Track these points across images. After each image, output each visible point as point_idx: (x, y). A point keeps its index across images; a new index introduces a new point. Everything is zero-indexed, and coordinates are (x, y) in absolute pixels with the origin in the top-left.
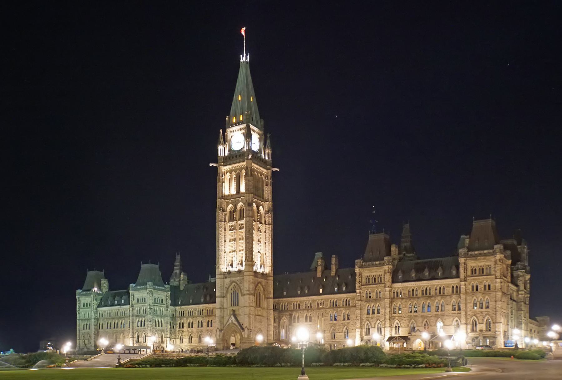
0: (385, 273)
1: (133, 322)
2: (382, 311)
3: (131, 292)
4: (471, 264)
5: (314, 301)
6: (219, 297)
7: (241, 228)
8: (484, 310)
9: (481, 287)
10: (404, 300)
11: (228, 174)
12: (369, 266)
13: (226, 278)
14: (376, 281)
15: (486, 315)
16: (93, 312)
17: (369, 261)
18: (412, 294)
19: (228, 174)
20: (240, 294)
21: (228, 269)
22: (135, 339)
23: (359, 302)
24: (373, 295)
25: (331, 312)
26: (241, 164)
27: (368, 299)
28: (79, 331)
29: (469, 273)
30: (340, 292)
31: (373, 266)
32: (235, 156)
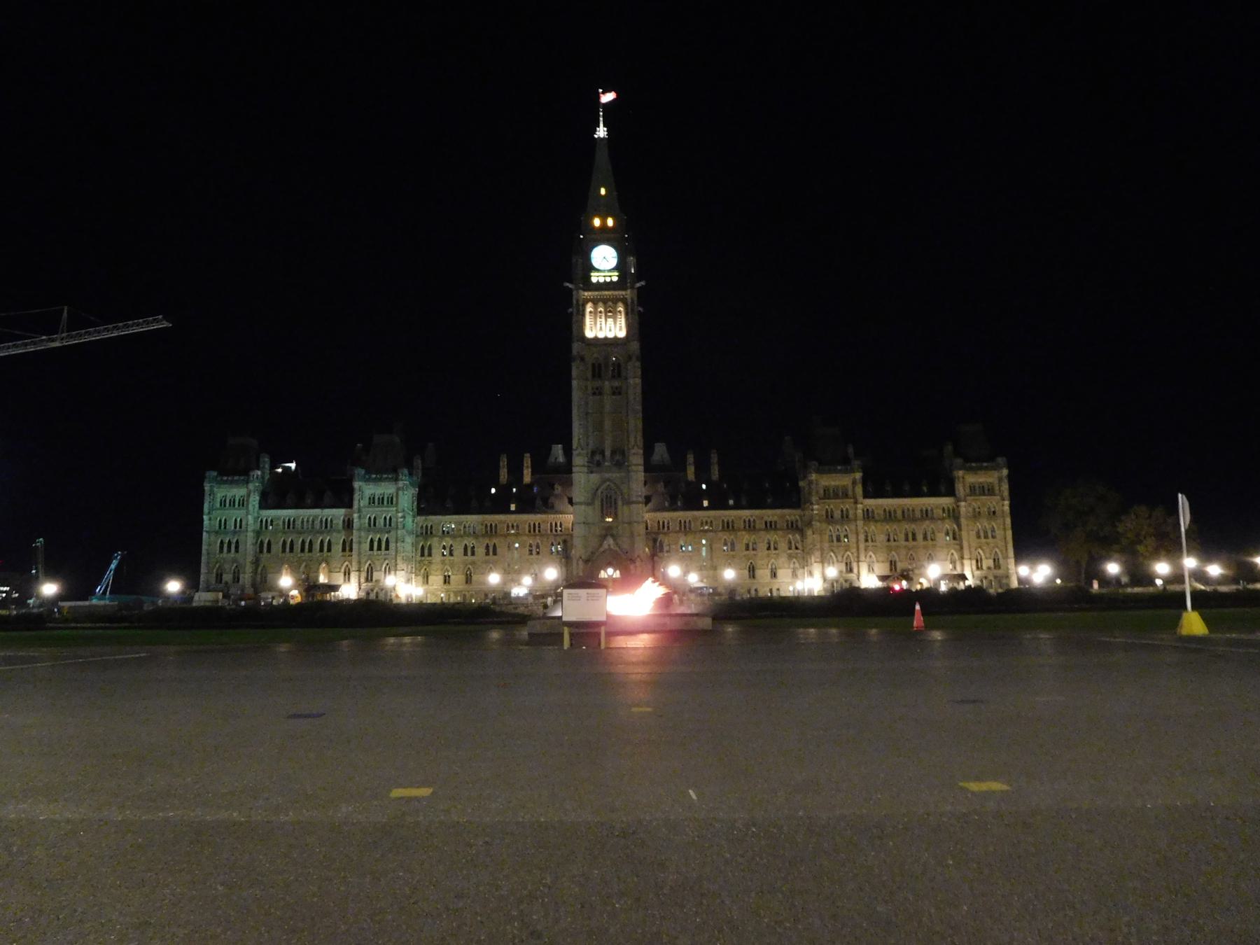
0: (854, 483)
1: (360, 543)
4: (971, 479)
5: (696, 519)
8: (990, 540)
10: (879, 524)
12: (829, 472)
17: (827, 465)
18: (889, 517)
20: (620, 503)
24: (837, 514)
25: (725, 536)
26: (616, 293)
27: (829, 518)
29: (968, 491)
30: (736, 507)
31: (836, 471)
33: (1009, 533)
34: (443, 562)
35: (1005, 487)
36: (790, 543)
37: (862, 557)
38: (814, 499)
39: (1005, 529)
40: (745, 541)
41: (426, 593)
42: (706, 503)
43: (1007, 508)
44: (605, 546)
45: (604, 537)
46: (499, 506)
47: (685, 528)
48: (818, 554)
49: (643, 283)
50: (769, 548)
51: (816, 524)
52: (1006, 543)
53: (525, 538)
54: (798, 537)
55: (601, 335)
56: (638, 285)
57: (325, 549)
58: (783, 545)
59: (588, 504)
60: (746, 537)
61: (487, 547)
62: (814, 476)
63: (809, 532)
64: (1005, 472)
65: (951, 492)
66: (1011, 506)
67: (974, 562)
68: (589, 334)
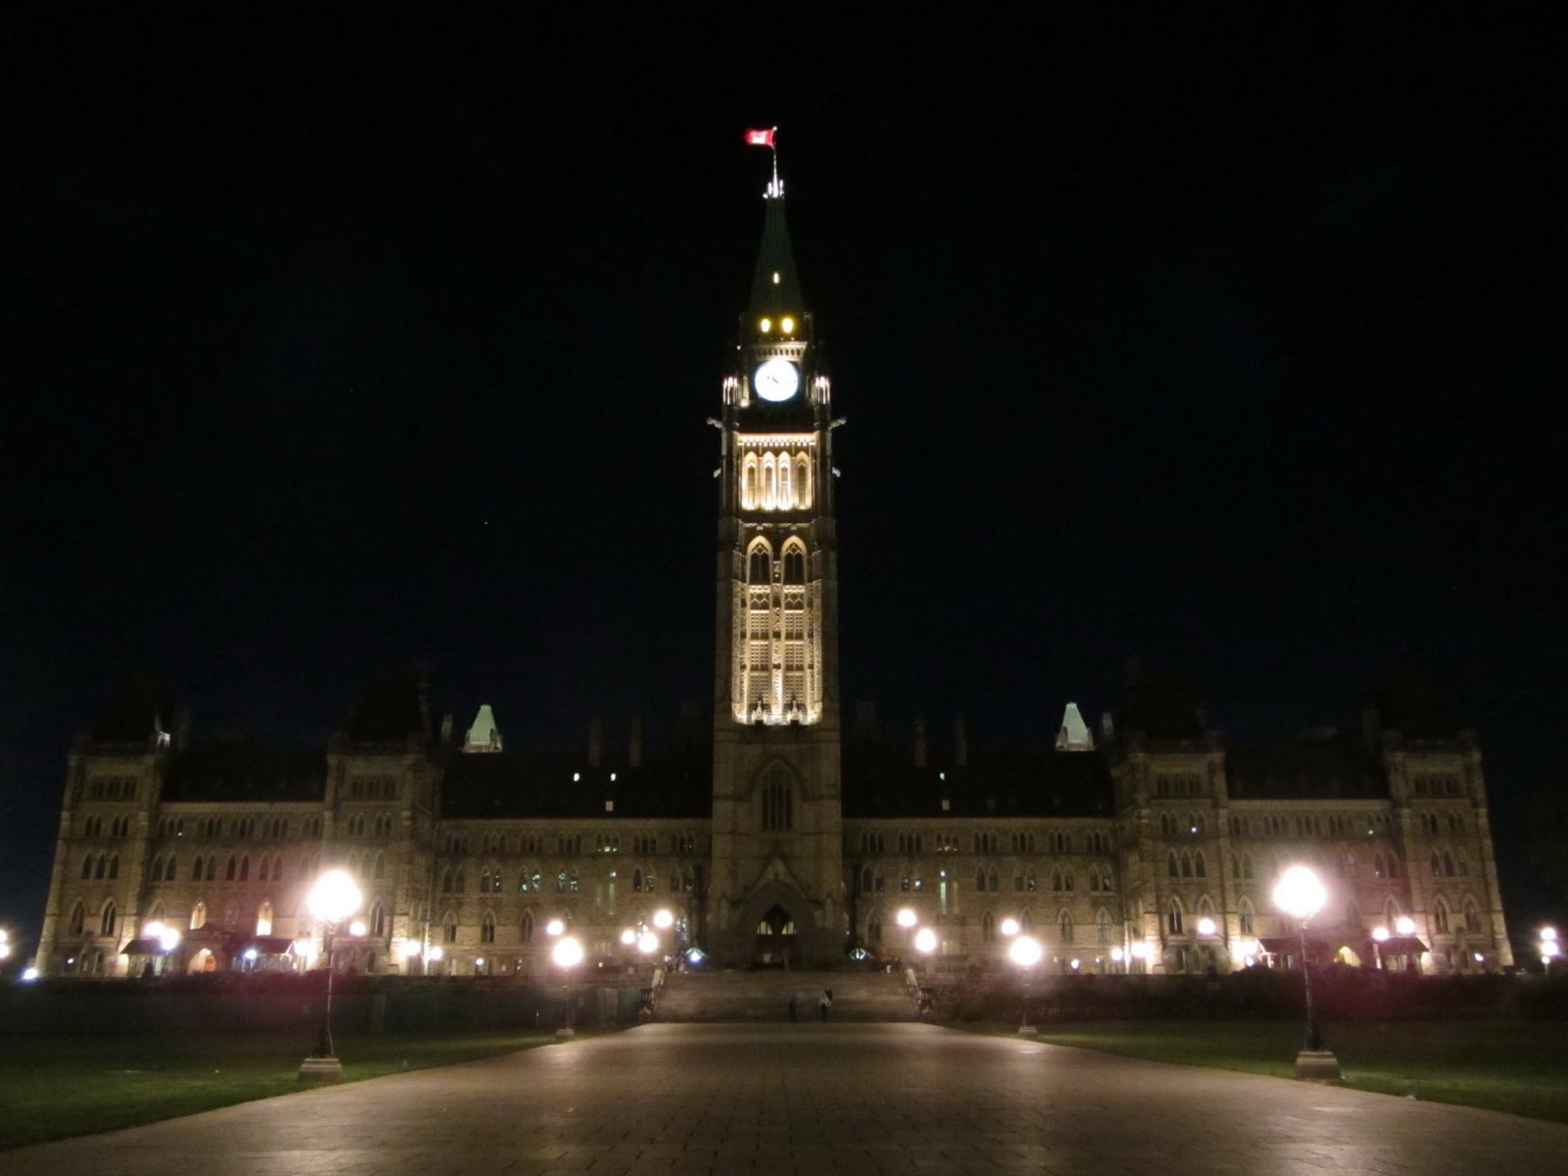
0: (1212, 770)
2: (1211, 868)
3: (332, 760)
6: (726, 797)
7: (789, 606)
9: (1443, 823)
11: (751, 456)
13: (748, 743)
14: (1189, 789)
15: (1465, 891)
16: (143, 815)
19: (751, 456)
21: (754, 717)
22: (68, 921)
23: (1150, 843)
27: (1169, 833)
28: (64, 881)
32: (766, 417)
33: (1492, 868)
34: (482, 903)
35: (1479, 781)
36: (1094, 879)
37: (1231, 907)
38: (1141, 798)
39: (1483, 860)
40: (1016, 873)
41: (449, 957)
42: (946, 805)
43: (1483, 821)
44: (771, 876)
45: (767, 860)
46: (585, 803)
47: (911, 849)
48: (1151, 898)
49: (842, 422)
50: (1057, 888)
51: (1148, 844)
52: (1487, 885)
53: (628, 861)
54: (1109, 868)
55: (769, 505)
56: (834, 425)
57: (107, 873)
58: (1083, 883)
59: (737, 798)
60: (1017, 866)
61: (199, 863)
62: (1141, 757)
63: (1133, 859)
64: (1476, 757)
65: (1381, 790)
66: (1492, 818)
67: (1432, 918)
68: (747, 504)
